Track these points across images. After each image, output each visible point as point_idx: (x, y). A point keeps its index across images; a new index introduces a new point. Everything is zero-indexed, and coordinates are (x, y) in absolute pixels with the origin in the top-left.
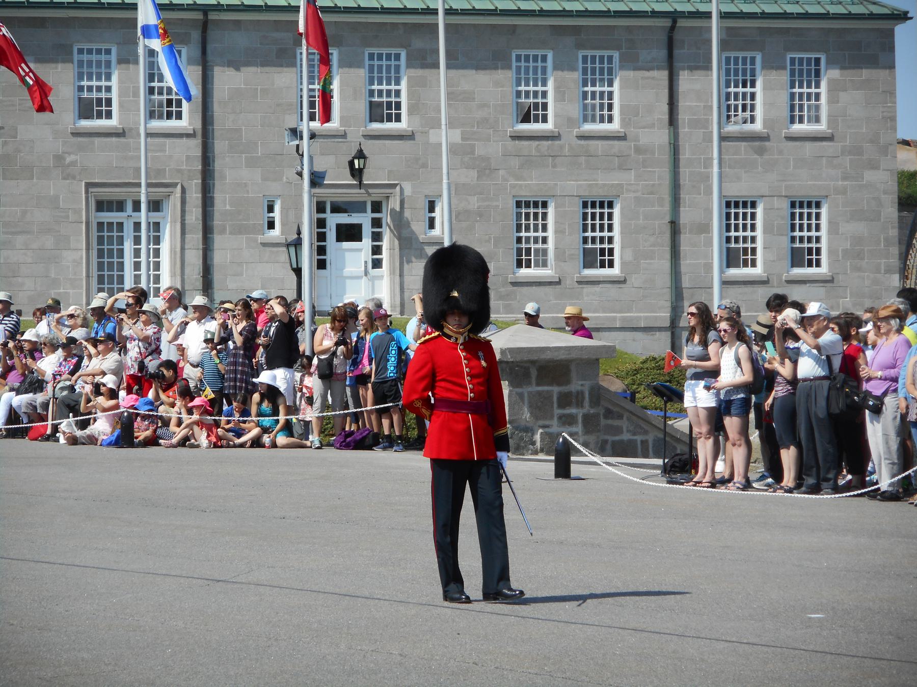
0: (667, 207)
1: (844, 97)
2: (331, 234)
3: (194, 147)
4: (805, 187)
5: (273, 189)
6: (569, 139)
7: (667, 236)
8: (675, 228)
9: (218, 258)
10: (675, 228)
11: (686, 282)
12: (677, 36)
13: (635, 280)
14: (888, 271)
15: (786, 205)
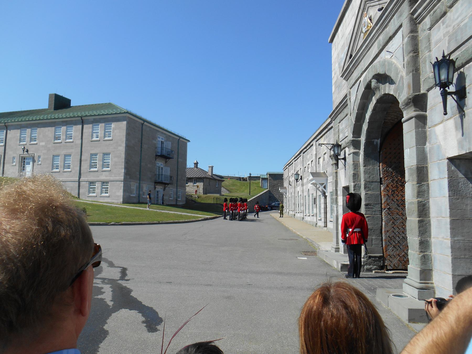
0: (79, 156)
1: (115, 131)
2: (25, 164)
3: (3, 147)
4: (106, 151)
5: (15, 155)
6: (63, 143)
7: (79, 163)
8: (81, 159)
9: (5, 168)
10: (81, 159)
11: (82, 172)
12: (84, 121)
13: (73, 172)
14: (122, 169)
15: (102, 155)
